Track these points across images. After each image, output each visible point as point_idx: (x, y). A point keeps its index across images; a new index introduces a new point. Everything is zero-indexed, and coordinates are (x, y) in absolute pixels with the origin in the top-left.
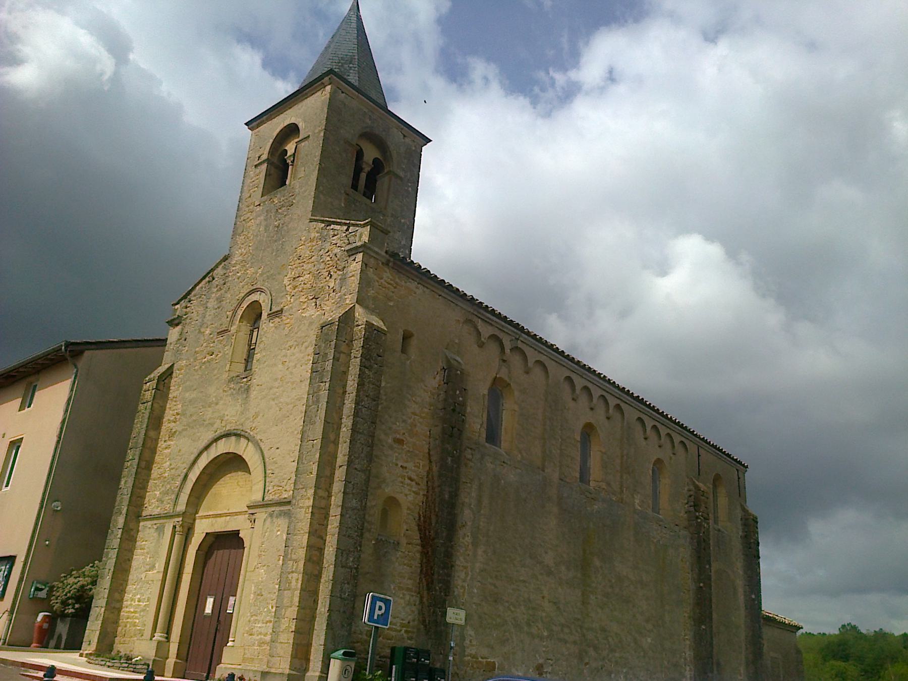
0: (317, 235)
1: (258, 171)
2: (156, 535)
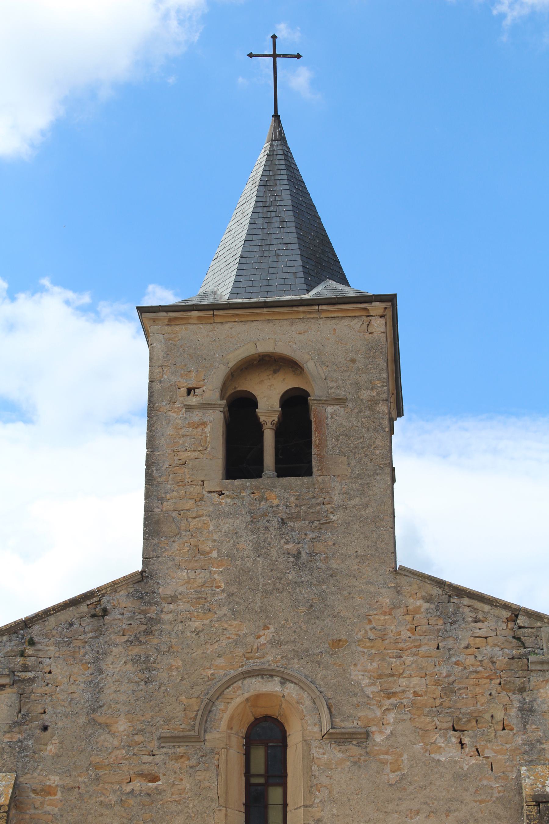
0: (426, 605)
1: (196, 417)
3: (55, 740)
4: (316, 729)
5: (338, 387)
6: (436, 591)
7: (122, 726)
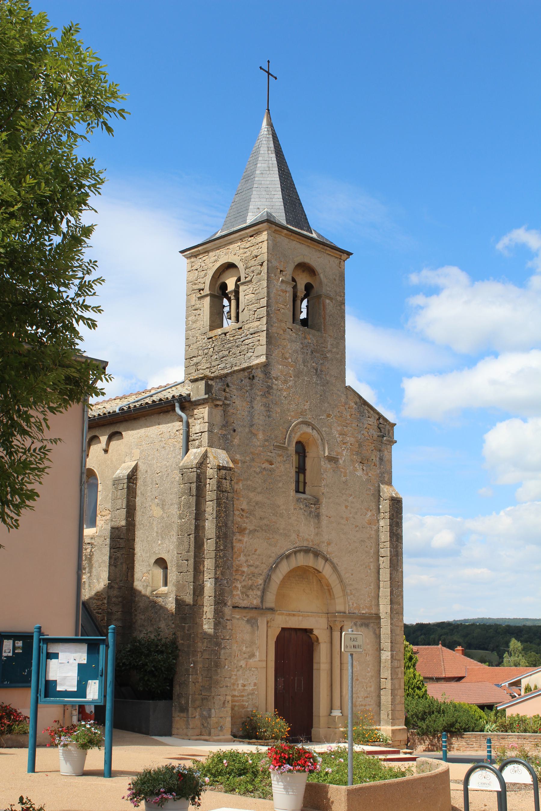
0: (355, 406)
2: (248, 627)
3: (238, 437)
4: (323, 453)
5: (330, 291)
6: (358, 400)
7: (261, 436)
